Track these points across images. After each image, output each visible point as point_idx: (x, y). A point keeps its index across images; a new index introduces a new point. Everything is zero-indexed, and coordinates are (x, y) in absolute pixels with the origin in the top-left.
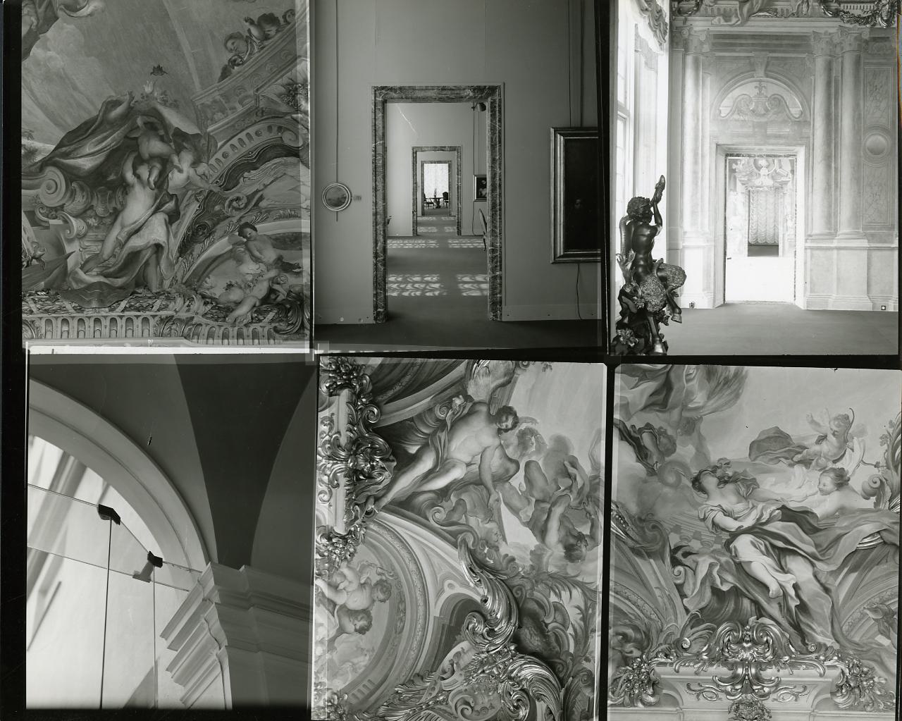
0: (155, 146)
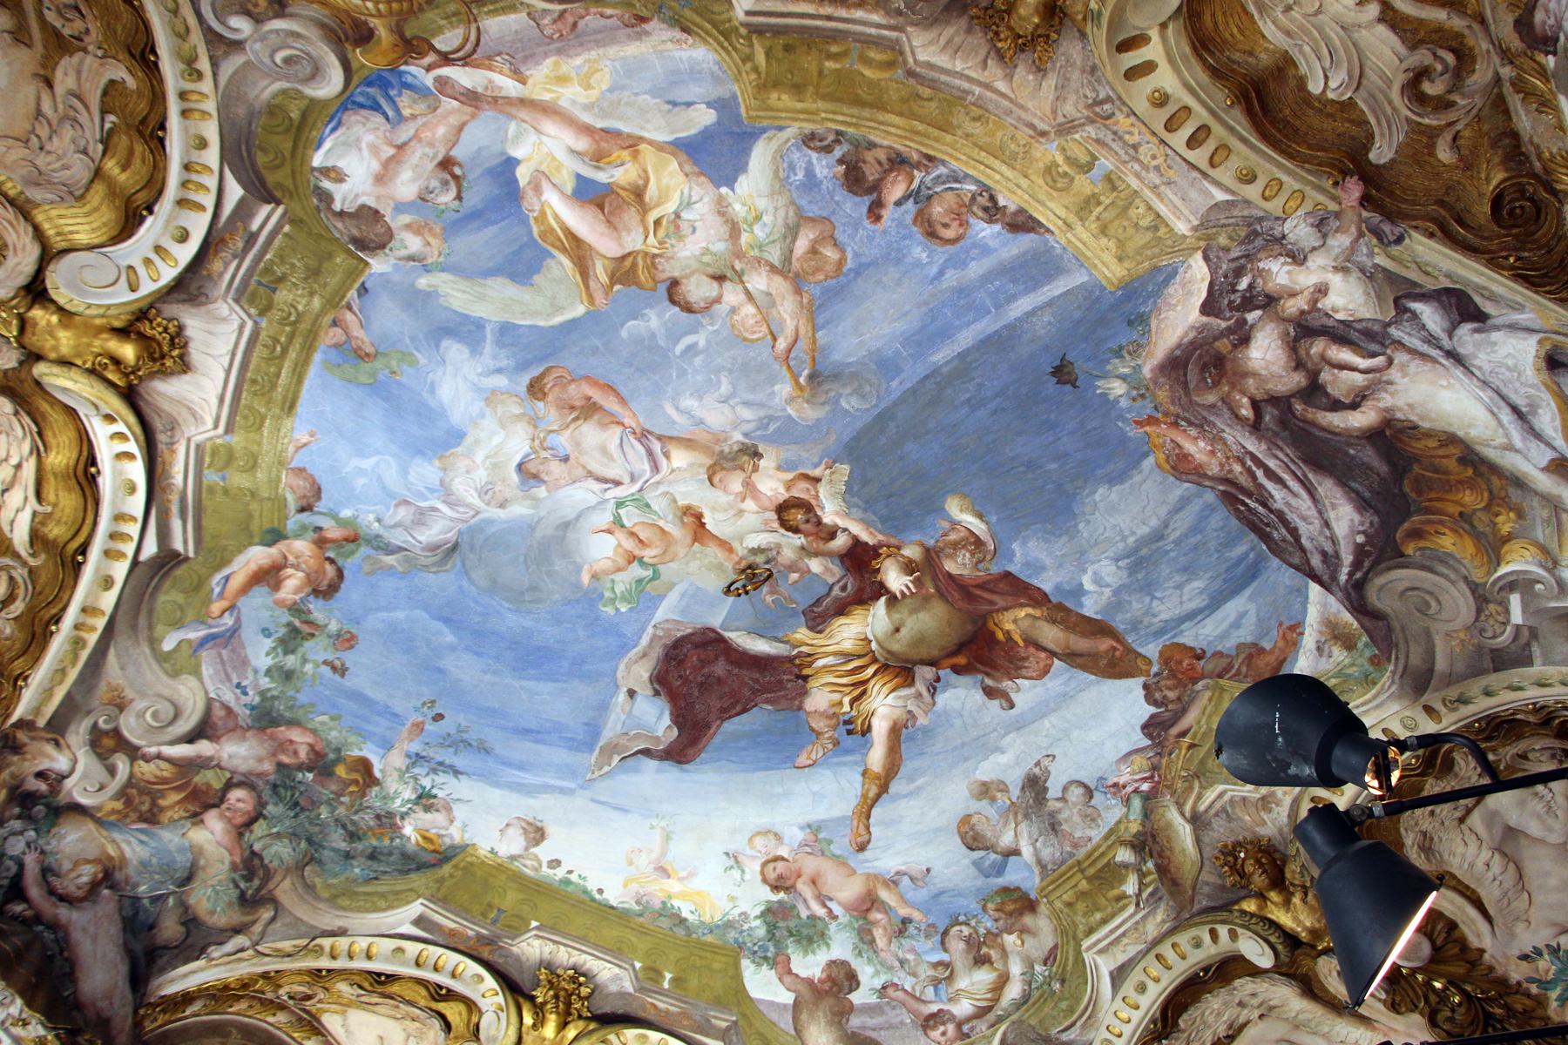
0: (1265, 353)
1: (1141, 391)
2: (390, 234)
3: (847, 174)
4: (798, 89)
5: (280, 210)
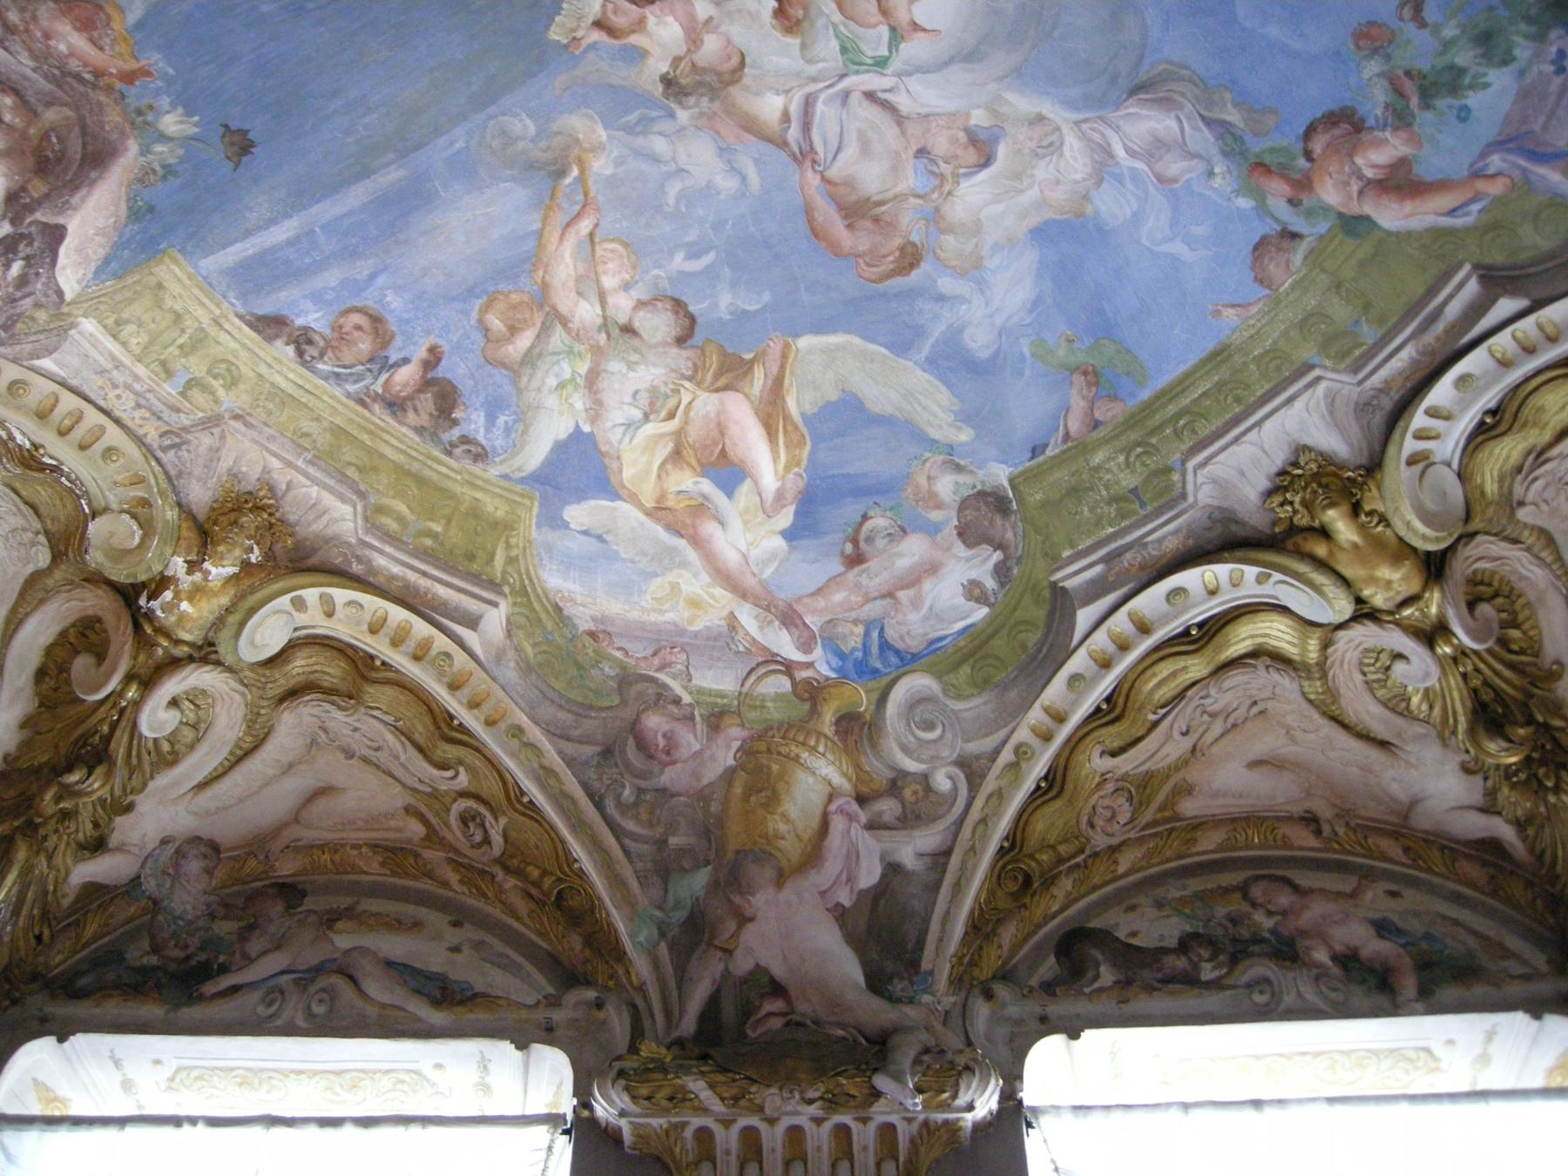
1: (142, 122)
2: (963, 505)
3: (453, 407)
4: (475, 513)
5: (1059, 575)
